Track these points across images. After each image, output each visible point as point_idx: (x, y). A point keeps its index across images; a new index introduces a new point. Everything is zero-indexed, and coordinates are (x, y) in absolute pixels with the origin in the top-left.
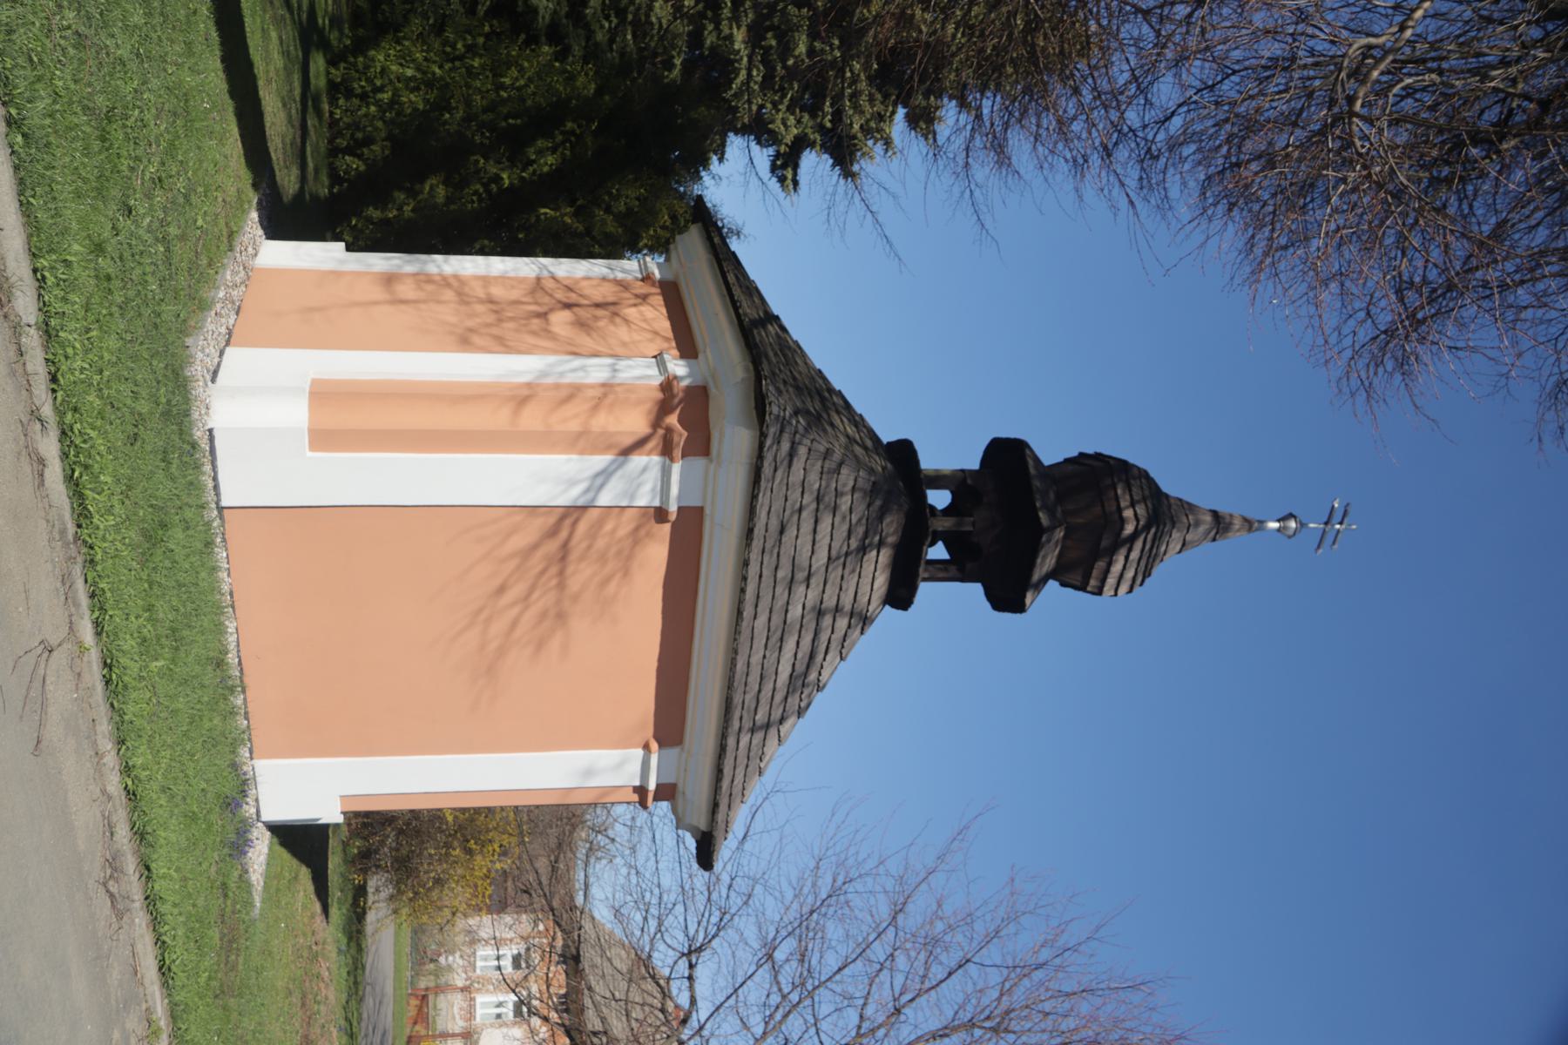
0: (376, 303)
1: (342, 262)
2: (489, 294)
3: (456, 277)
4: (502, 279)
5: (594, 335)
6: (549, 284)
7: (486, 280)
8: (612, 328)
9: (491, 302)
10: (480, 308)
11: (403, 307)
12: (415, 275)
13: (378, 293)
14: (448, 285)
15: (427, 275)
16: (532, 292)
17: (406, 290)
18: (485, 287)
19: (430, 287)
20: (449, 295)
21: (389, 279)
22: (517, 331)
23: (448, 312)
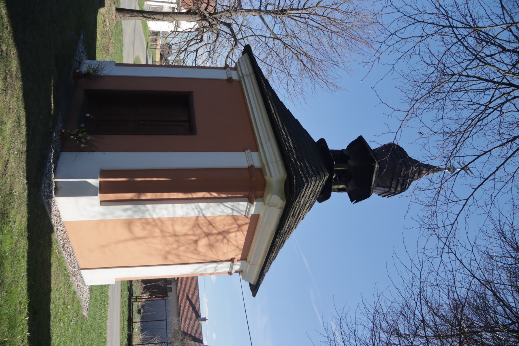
0: (127, 240)
1: (103, 214)
2: (174, 231)
3: (159, 219)
4: (183, 220)
5: (213, 250)
6: (202, 221)
7: (173, 220)
8: (222, 245)
9: (176, 235)
10: (171, 239)
11: (140, 241)
12: (140, 219)
13: (124, 234)
14: (156, 225)
15: (146, 219)
16: (194, 227)
17: (138, 231)
18: (173, 225)
19: (148, 227)
20: (157, 232)
21: (129, 224)
22: (185, 251)
23: (157, 244)
